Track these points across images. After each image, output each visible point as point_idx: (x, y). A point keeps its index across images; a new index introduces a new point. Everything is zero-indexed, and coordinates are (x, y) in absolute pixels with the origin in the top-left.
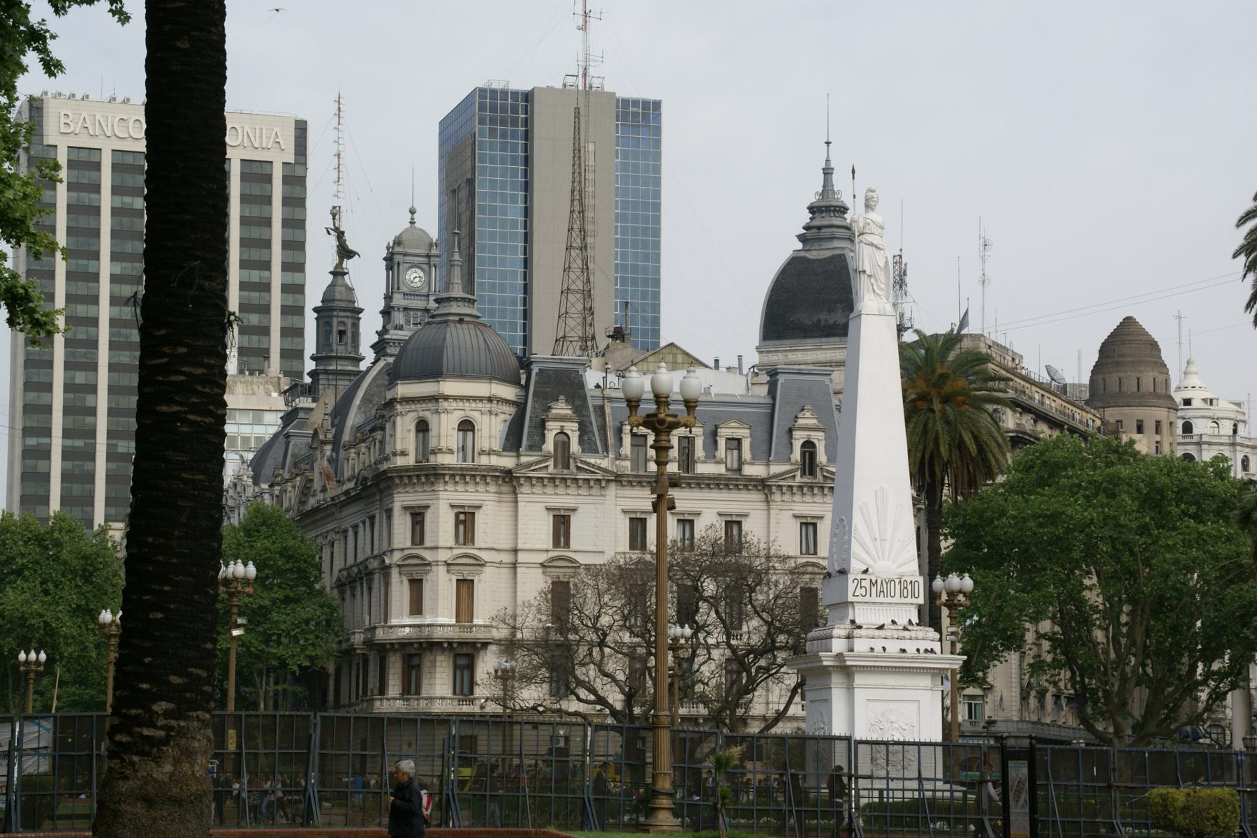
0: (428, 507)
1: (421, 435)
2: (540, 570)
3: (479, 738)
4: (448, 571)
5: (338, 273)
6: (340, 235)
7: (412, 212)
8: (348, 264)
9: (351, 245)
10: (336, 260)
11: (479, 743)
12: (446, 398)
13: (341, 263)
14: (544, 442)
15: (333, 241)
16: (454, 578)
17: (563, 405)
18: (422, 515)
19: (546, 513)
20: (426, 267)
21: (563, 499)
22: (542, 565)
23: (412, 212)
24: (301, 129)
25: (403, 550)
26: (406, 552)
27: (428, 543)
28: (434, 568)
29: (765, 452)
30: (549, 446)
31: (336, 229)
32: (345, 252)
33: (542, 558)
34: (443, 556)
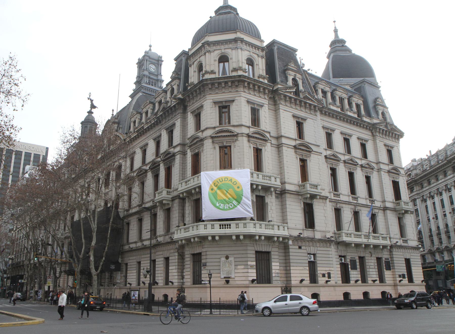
0: (233, 101)
1: (221, 65)
2: (293, 150)
3: (272, 253)
4: (249, 141)
5: (90, 112)
6: (92, 101)
7: (150, 46)
8: (93, 110)
9: (95, 104)
10: (90, 109)
11: (273, 257)
12: (242, 41)
13: (91, 109)
14: (287, 81)
15: (89, 102)
16: (252, 146)
17: (293, 65)
18: (228, 107)
19: (292, 118)
20: (157, 65)
21: (301, 113)
22: (295, 147)
23: (150, 46)
24: (47, 148)
25: (214, 128)
26: (217, 129)
27: (233, 122)
28: (240, 138)
29: (369, 114)
30: (290, 83)
31: (91, 100)
32: (93, 106)
33: (293, 143)
34: (245, 131)
